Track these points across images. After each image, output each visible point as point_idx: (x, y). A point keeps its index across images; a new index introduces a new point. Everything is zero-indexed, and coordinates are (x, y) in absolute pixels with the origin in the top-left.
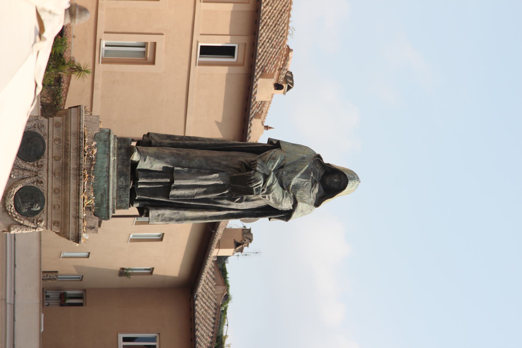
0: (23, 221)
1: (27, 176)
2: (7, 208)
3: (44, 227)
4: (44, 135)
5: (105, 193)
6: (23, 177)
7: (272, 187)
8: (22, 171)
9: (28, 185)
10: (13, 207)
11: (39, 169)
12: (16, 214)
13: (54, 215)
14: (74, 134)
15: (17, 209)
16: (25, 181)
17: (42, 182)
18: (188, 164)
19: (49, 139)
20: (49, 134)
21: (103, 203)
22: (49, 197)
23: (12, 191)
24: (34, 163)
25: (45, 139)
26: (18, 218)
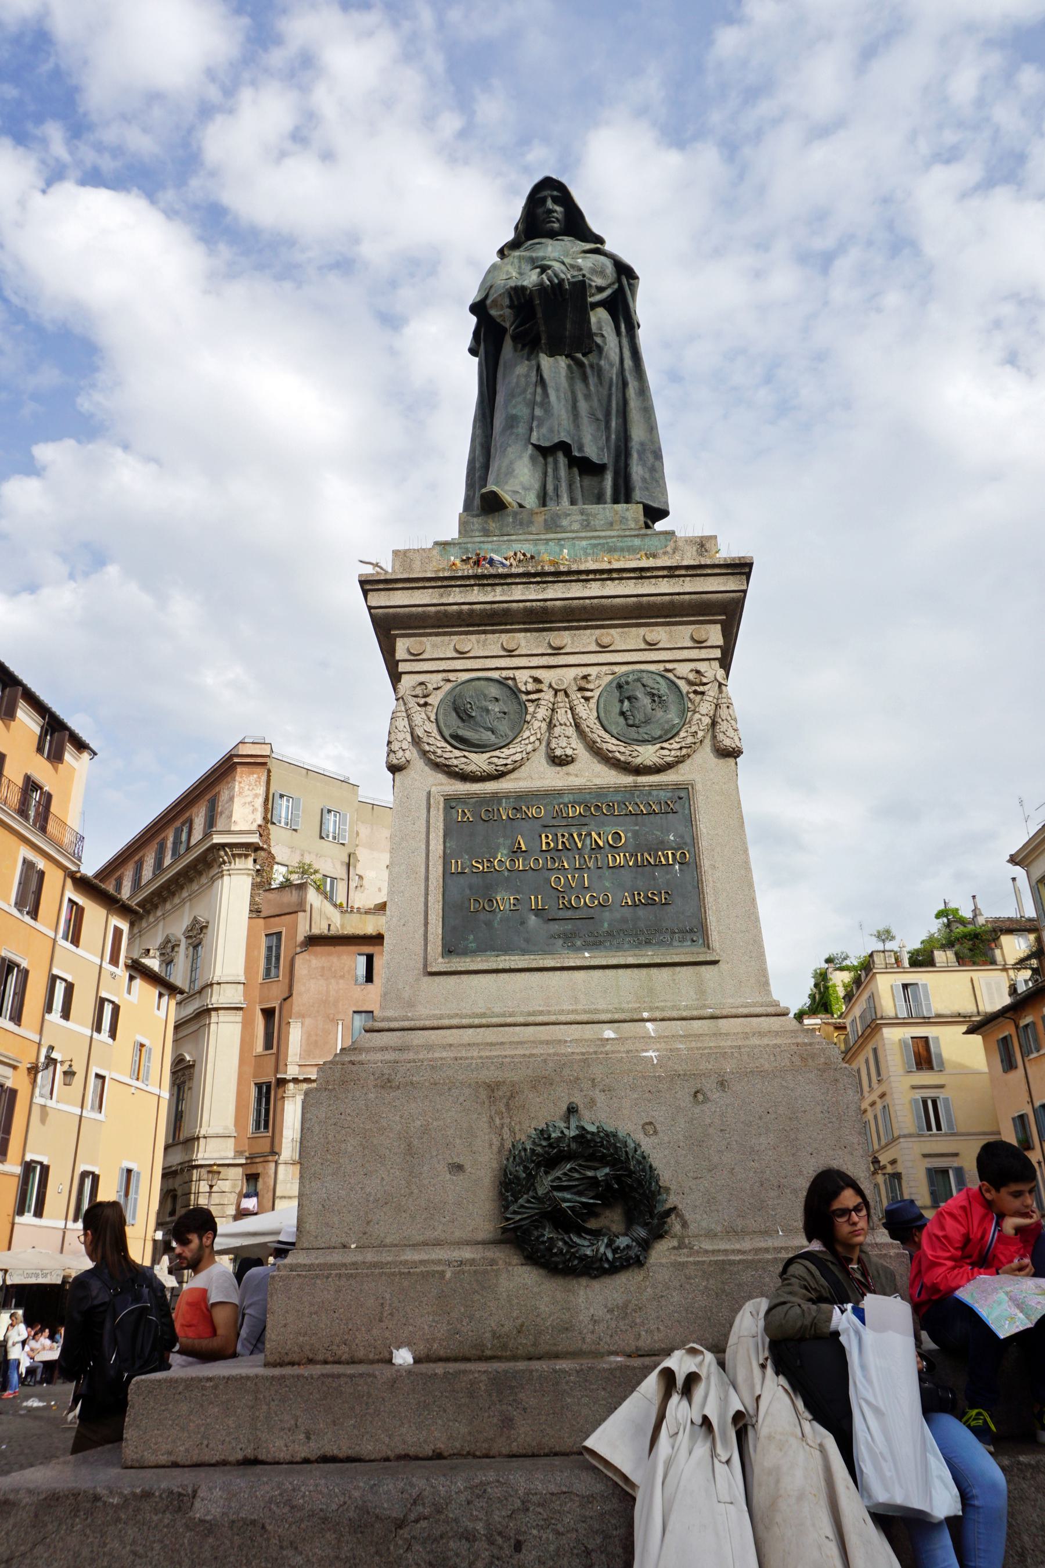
1: (570, 716)
2: (669, 759)
4: (449, 681)
5: (604, 544)
9: (595, 714)
10: (665, 745)
11: (545, 689)
12: (682, 734)
13: (676, 643)
14: (441, 596)
15: (670, 736)
17: (585, 677)
20: (444, 671)
23: (614, 748)
24: (528, 701)
25: (459, 680)
26: (694, 729)
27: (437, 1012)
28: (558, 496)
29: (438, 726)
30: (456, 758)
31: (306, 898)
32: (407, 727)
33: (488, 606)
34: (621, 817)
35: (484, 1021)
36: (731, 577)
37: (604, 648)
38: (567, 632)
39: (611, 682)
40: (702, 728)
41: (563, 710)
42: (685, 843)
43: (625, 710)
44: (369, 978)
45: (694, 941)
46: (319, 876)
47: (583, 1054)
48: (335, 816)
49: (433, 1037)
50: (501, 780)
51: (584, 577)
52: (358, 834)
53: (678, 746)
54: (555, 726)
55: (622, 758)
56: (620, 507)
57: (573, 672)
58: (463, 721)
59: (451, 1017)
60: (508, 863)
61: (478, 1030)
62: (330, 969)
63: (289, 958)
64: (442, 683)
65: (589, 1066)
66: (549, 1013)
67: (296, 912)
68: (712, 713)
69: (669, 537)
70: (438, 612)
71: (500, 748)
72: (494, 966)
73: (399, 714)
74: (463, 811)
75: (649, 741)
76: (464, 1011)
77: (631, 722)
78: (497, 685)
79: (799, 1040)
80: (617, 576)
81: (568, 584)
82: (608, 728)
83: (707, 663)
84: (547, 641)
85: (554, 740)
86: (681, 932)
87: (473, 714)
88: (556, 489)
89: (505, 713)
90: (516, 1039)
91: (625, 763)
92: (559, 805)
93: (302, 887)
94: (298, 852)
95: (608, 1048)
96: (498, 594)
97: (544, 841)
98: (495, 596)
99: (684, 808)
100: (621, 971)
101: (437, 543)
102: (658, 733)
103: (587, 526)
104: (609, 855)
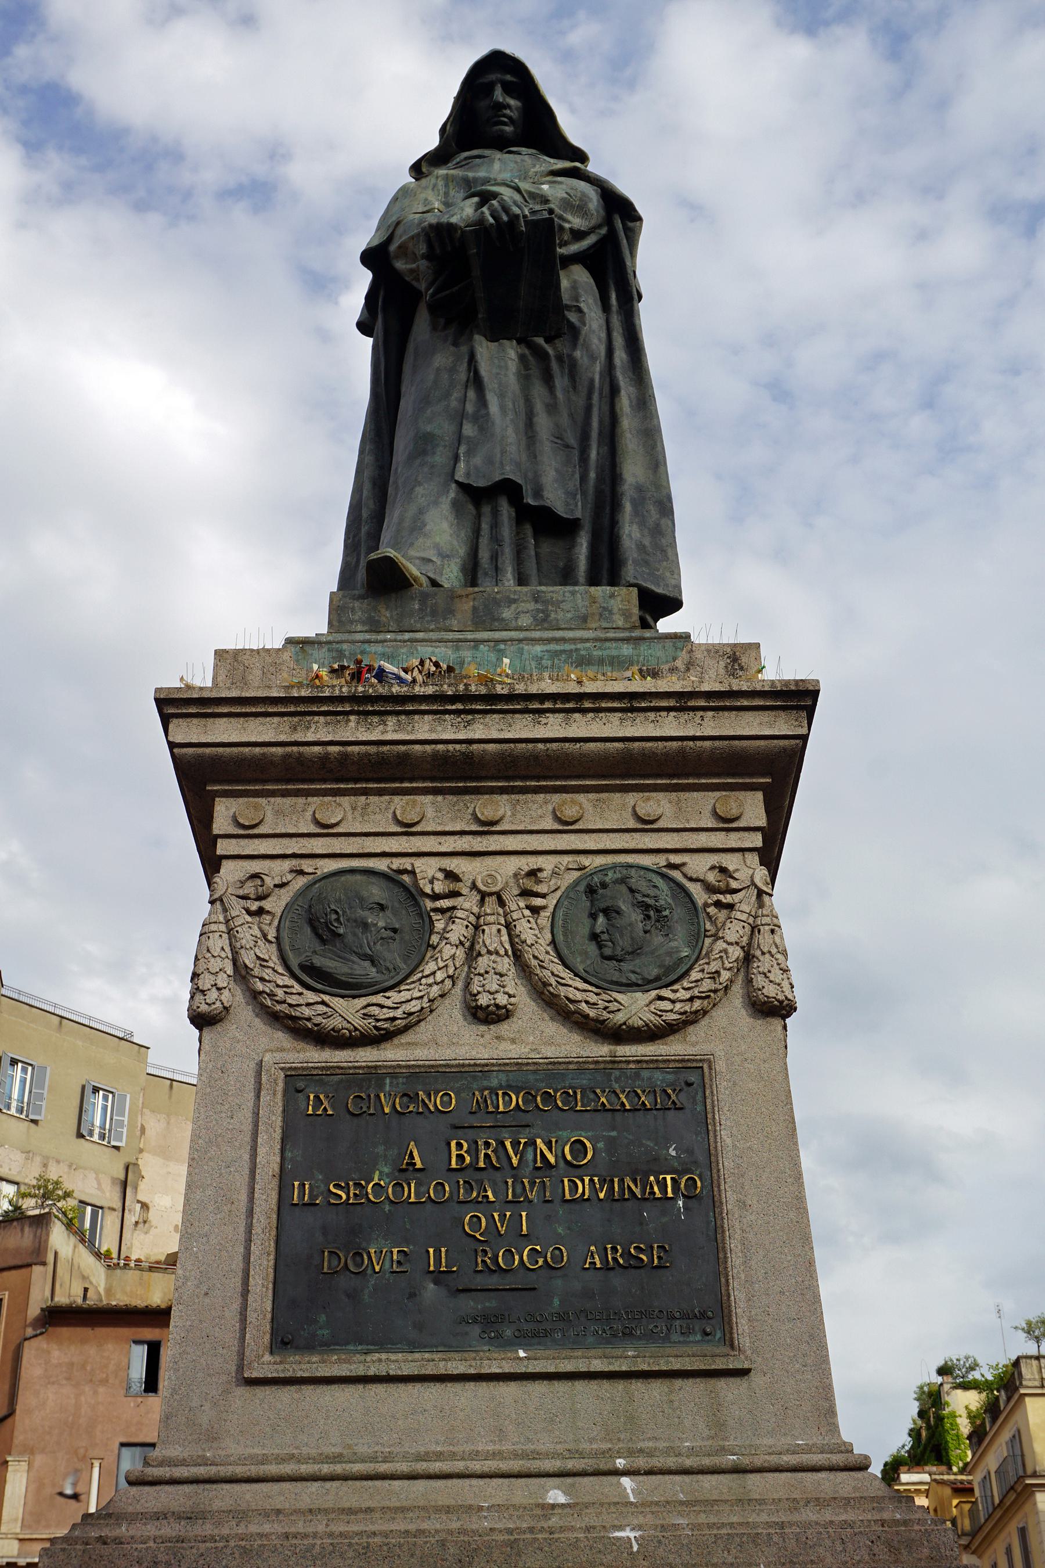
0: (731, 944)
1: (505, 938)
3: (748, 863)
4: (301, 872)
5: (571, 651)
6: (506, 951)
7: (526, 191)
8: (480, 959)
9: (549, 936)
10: (666, 993)
11: (465, 891)
12: (695, 975)
13: (688, 821)
14: (294, 729)
16: (529, 942)
17: (533, 873)
18: (445, 446)
19: (320, 851)
20: (294, 856)
21: (618, 657)
22: (600, 846)
23: (579, 996)
24: (436, 910)
25: (319, 872)
26: (714, 966)
27: (258, 1451)
28: (497, 569)
29: (280, 950)
30: (308, 1005)
31: (47, 1241)
32: (227, 949)
33: (372, 749)
34: (587, 1115)
35: (338, 1469)
36: (782, 713)
37: (566, 826)
38: (505, 797)
39: (577, 883)
40: (728, 965)
41: (495, 928)
42: (695, 1162)
43: (598, 931)
44: (151, 1384)
45: (707, 1334)
46: (72, 1203)
47: (510, 1532)
48: (106, 1098)
49: (248, 1497)
50: (387, 1045)
51: (536, 706)
52: (143, 1130)
53: (688, 996)
54: (479, 954)
55: (592, 1013)
56: (598, 591)
57: (513, 864)
58: (323, 941)
59: (281, 1460)
60: (390, 1190)
61: (328, 1485)
62: (83, 1367)
63: (12, 1347)
64: (289, 877)
65: (519, 1555)
66: (453, 1457)
67: (29, 1265)
68: (745, 941)
69: (679, 644)
70: (288, 756)
71: (385, 990)
72: (360, 1371)
73: (213, 927)
74: (317, 1097)
75: (638, 985)
76: (305, 1450)
77: (608, 952)
78: (383, 883)
79: (886, 1515)
80: (591, 705)
81: (509, 716)
82: (570, 960)
83: (739, 855)
84: (470, 810)
85: (476, 979)
86: (685, 1316)
87: (341, 931)
88: (495, 557)
89: (395, 931)
90: (394, 1503)
91: (596, 1020)
92: (482, 1091)
93: (41, 1221)
94: (38, 1159)
95: (554, 1521)
96: (390, 730)
97: (454, 1152)
98: (384, 732)
99: (694, 1102)
100: (579, 1385)
101: (290, 641)
102: (655, 972)
103: (544, 620)
104: (566, 1180)
